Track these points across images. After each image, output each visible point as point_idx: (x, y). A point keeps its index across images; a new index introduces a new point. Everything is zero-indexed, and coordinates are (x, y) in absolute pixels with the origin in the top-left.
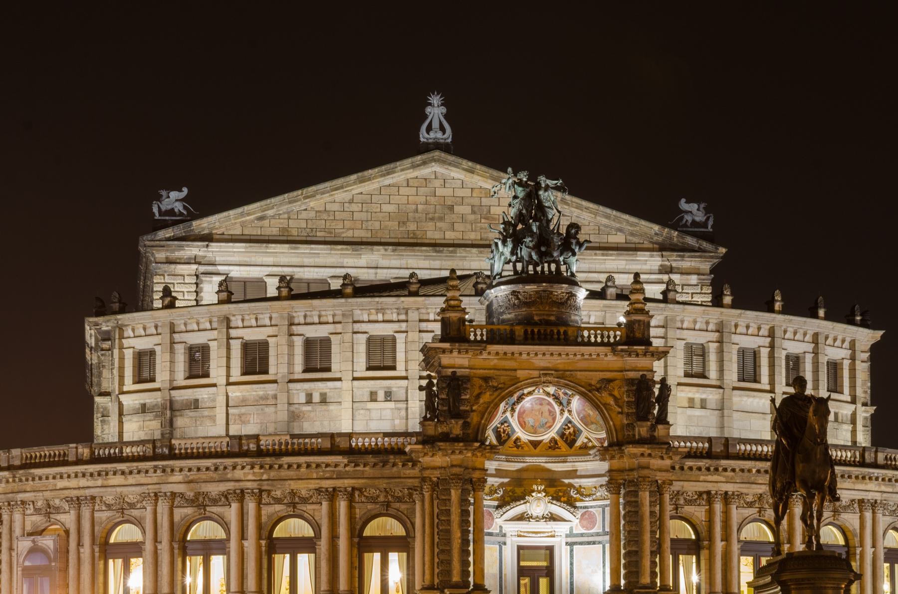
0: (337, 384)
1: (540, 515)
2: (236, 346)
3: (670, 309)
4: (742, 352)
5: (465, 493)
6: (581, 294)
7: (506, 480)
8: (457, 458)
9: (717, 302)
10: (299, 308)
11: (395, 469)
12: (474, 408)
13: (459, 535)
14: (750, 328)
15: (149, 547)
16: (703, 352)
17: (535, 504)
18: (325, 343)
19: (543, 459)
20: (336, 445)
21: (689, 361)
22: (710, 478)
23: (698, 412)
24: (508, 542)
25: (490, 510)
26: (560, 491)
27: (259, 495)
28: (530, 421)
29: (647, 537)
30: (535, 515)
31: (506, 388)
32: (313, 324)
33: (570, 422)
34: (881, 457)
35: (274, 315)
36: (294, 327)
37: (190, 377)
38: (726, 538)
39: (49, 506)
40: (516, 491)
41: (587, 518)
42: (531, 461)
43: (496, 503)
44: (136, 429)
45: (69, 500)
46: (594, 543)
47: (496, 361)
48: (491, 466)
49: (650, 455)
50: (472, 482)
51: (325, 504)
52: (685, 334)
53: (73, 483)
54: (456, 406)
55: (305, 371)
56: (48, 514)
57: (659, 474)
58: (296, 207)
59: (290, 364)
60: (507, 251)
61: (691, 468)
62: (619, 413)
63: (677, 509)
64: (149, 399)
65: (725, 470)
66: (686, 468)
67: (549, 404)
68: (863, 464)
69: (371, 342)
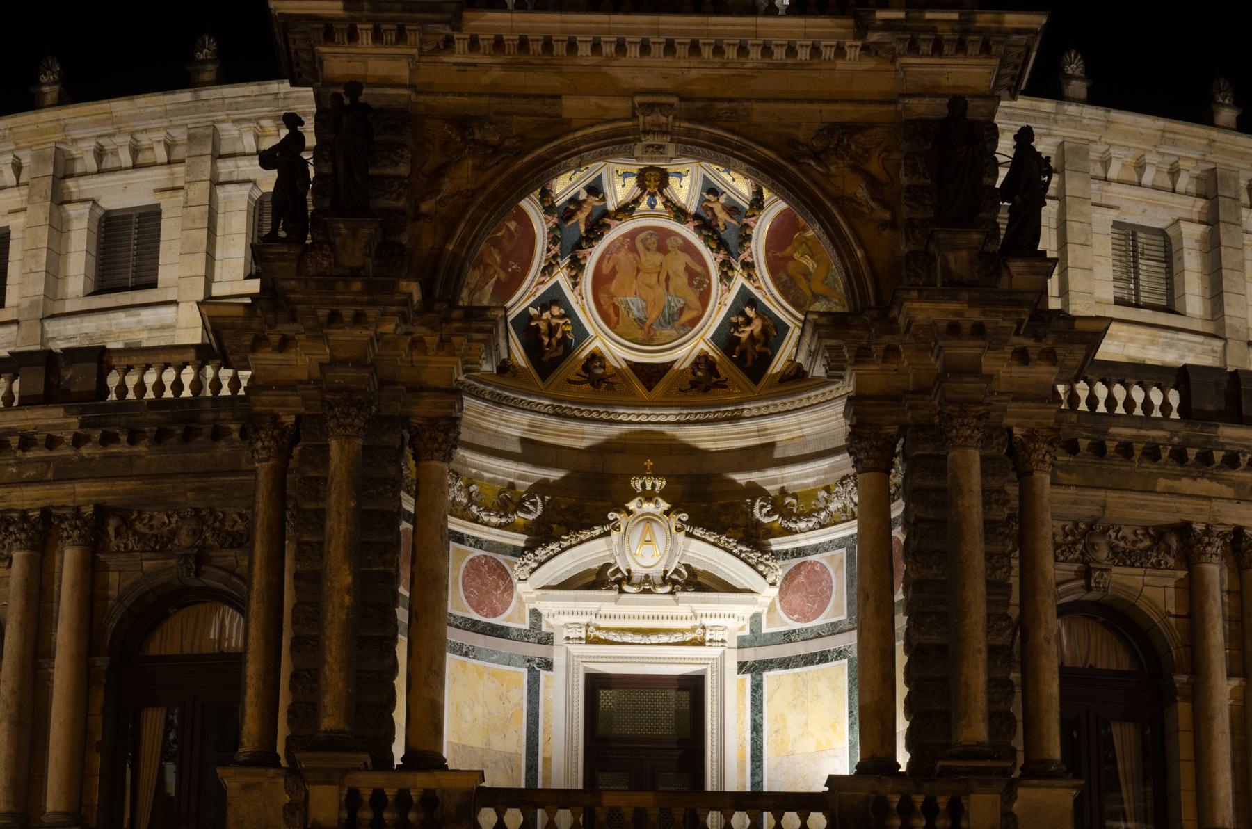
0: (167, 314)
1: (656, 573)
3: (1071, 118)
7: (555, 475)
11: (222, 447)
12: (425, 207)
13: (347, 579)
17: (636, 534)
18: (150, 218)
19: (671, 414)
22: (1186, 485)
24: (559, 659)
25: (501, 558)
26: (717, 502)
28: (632, 303)
30: (638, 573)
31: (524, 147)
32: (121, 169)
33: (753, 302)
35: (26, 161)
36: (70, 183)
40: (579, 500)
41: (802, 582)
42: (634, 419)
43: (519, 540)
46: (823, 658)
47: (497, 73)
48: (513, 425)
49: (978, 330)
51: (18, 556)
52: (1116, 193)
57: (1013, 407)
61: (1126, 449)
62: (884, 224)
63: (1086, 574)
65: (1232, 461)
66: (1111, 446)
67: (688, 248)
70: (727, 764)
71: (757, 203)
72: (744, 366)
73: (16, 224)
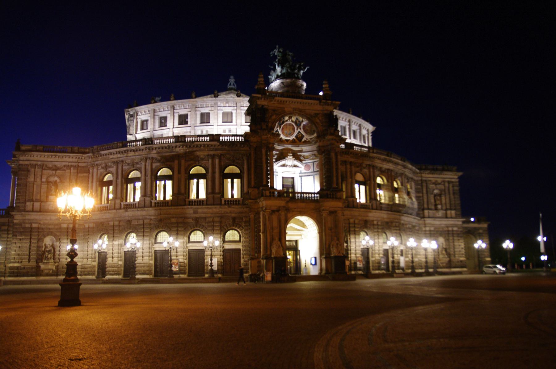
5: (267, 152)
15: (143, 178)
18: (208, 114)
19: (290, 146)
26: (297, 157)
35: (190, 105)
37: (161, 127)
39: (106, 166)
40: (282, 156)
41: (307, 166)
45: (114, 163)
51: (210, 160)
53: (115, 156)
55: (201, 123)
56: (106, 169)
65: (351, 153)
67: (293, 126)
70: (298, 189)
71: (303, 121)
72: (299, 140)
73: (189, 113)
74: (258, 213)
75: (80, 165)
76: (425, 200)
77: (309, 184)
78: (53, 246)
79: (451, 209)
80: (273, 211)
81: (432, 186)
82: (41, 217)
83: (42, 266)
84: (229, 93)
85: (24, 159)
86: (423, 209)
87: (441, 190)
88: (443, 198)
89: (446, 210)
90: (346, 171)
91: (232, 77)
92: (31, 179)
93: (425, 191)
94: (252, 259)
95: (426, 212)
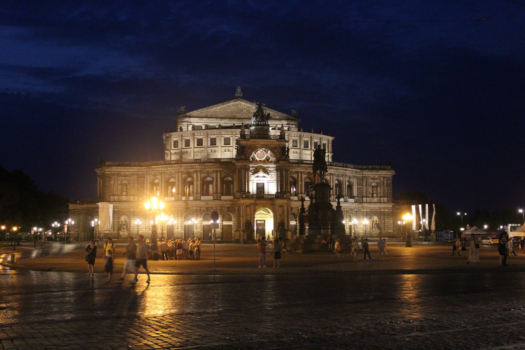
2: (196, 140)
4: (305, 141)
6: (270, 128)
8: (243, 164)
9: (299, 130)
10: (210, 131)
14: (306, 137)
16: (296, 141)
18: (215, 139)
20: (218, 161)
21: (293, 143)
23: (295, 154)
26: (265, 171)
27: (201, 172)
28: (259, 156)
29: (284, 181)
31: (255, 149)
34: (334, 164)
38: (301, 181)
40: (256, 171)
41: (272, 177)
44: (174, 158)
45: (160, 173)
48: (251, 165)
50: (247, 169)
53: (160, 169)
54: (244, 152)
58: (209, 110)
59: (207, 144)
60: (254, 119)
64: (176, 151)
68: (330, 165)
69: (225, 139)
72: (267, 160)
74: (240, 206)
75: (140, 173)
76: (365, 191)
77: (271, 188)
78: (125, 221)
79: (384, 197)
80: (247, 206)
81: (369, 181)
82: (119, 205)
83: (121, 233)
84: (236, 101)
85: (108, 171)
86: (362, 197)
87: (377, 183)
88: (379, 188)
89: (380, 197)
90: (298, 178)
91: (239, 87)
92: (112, 182)
93: (364, 184)
94: (236, 231)
95: (365, 199)
